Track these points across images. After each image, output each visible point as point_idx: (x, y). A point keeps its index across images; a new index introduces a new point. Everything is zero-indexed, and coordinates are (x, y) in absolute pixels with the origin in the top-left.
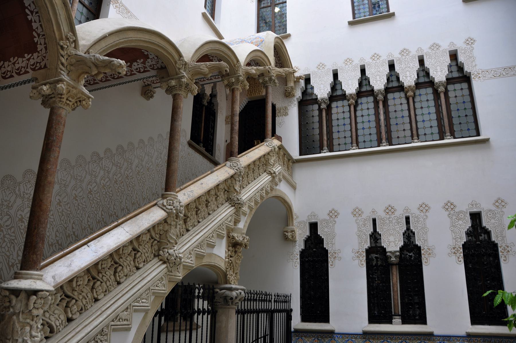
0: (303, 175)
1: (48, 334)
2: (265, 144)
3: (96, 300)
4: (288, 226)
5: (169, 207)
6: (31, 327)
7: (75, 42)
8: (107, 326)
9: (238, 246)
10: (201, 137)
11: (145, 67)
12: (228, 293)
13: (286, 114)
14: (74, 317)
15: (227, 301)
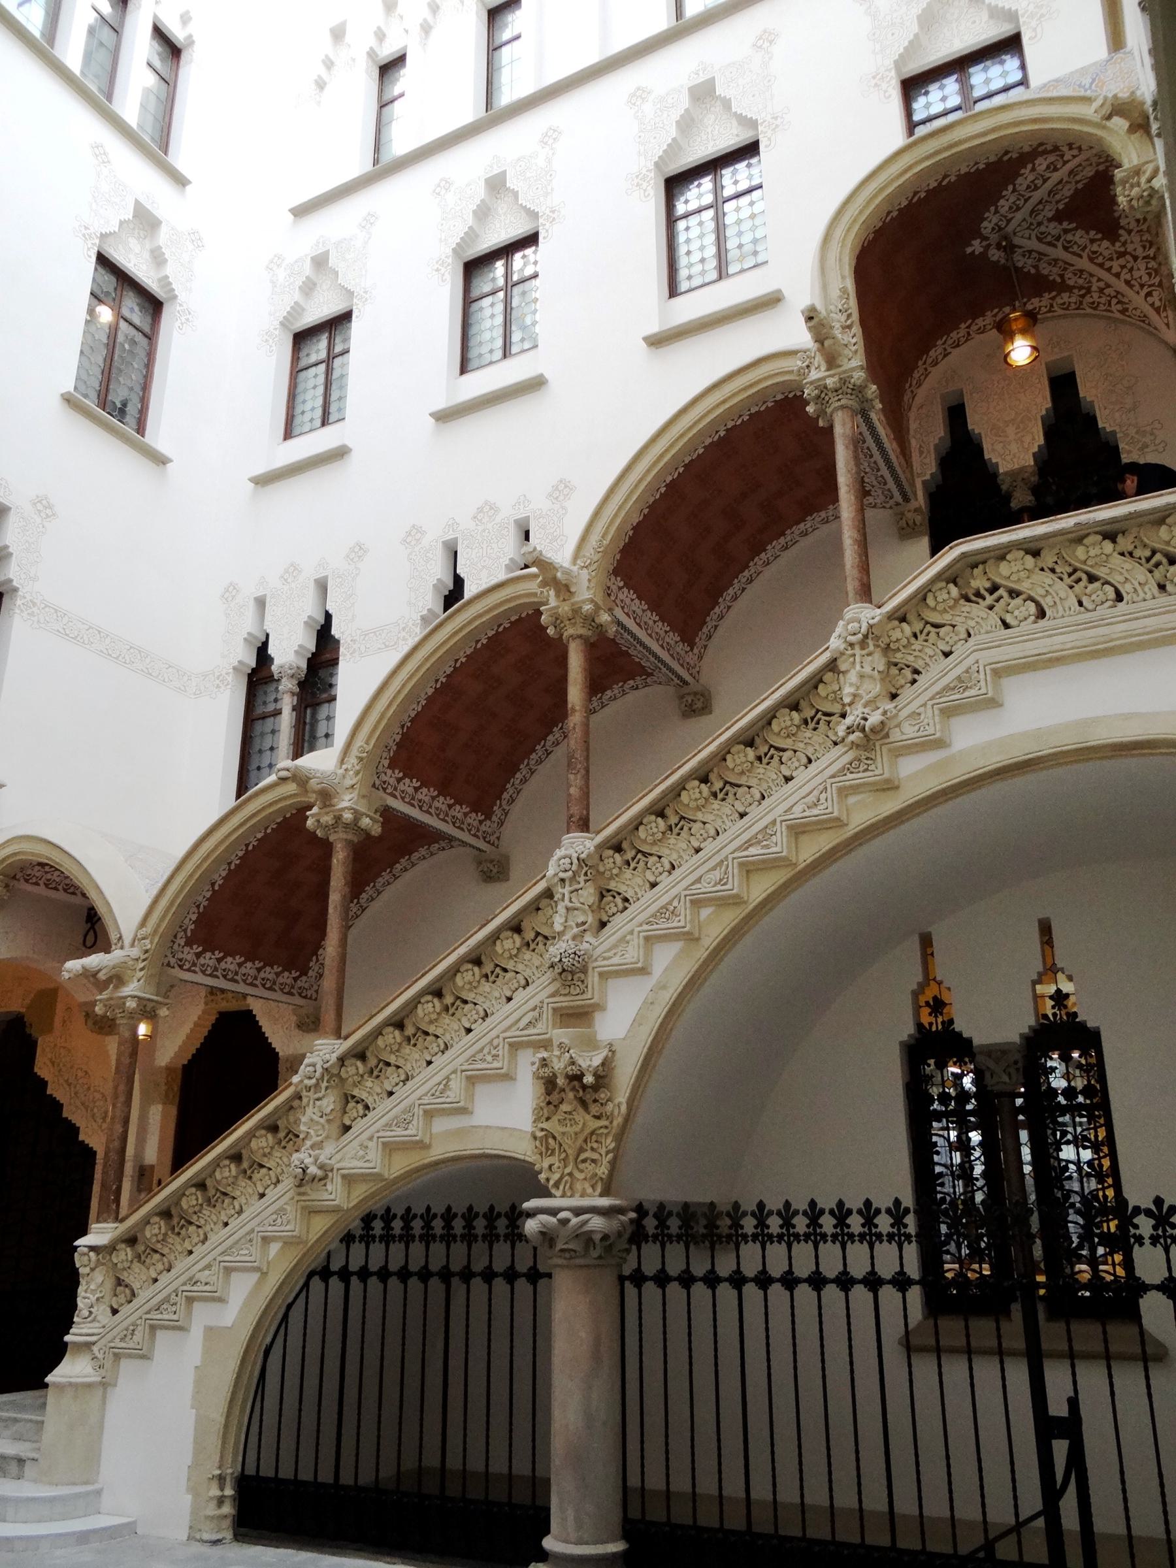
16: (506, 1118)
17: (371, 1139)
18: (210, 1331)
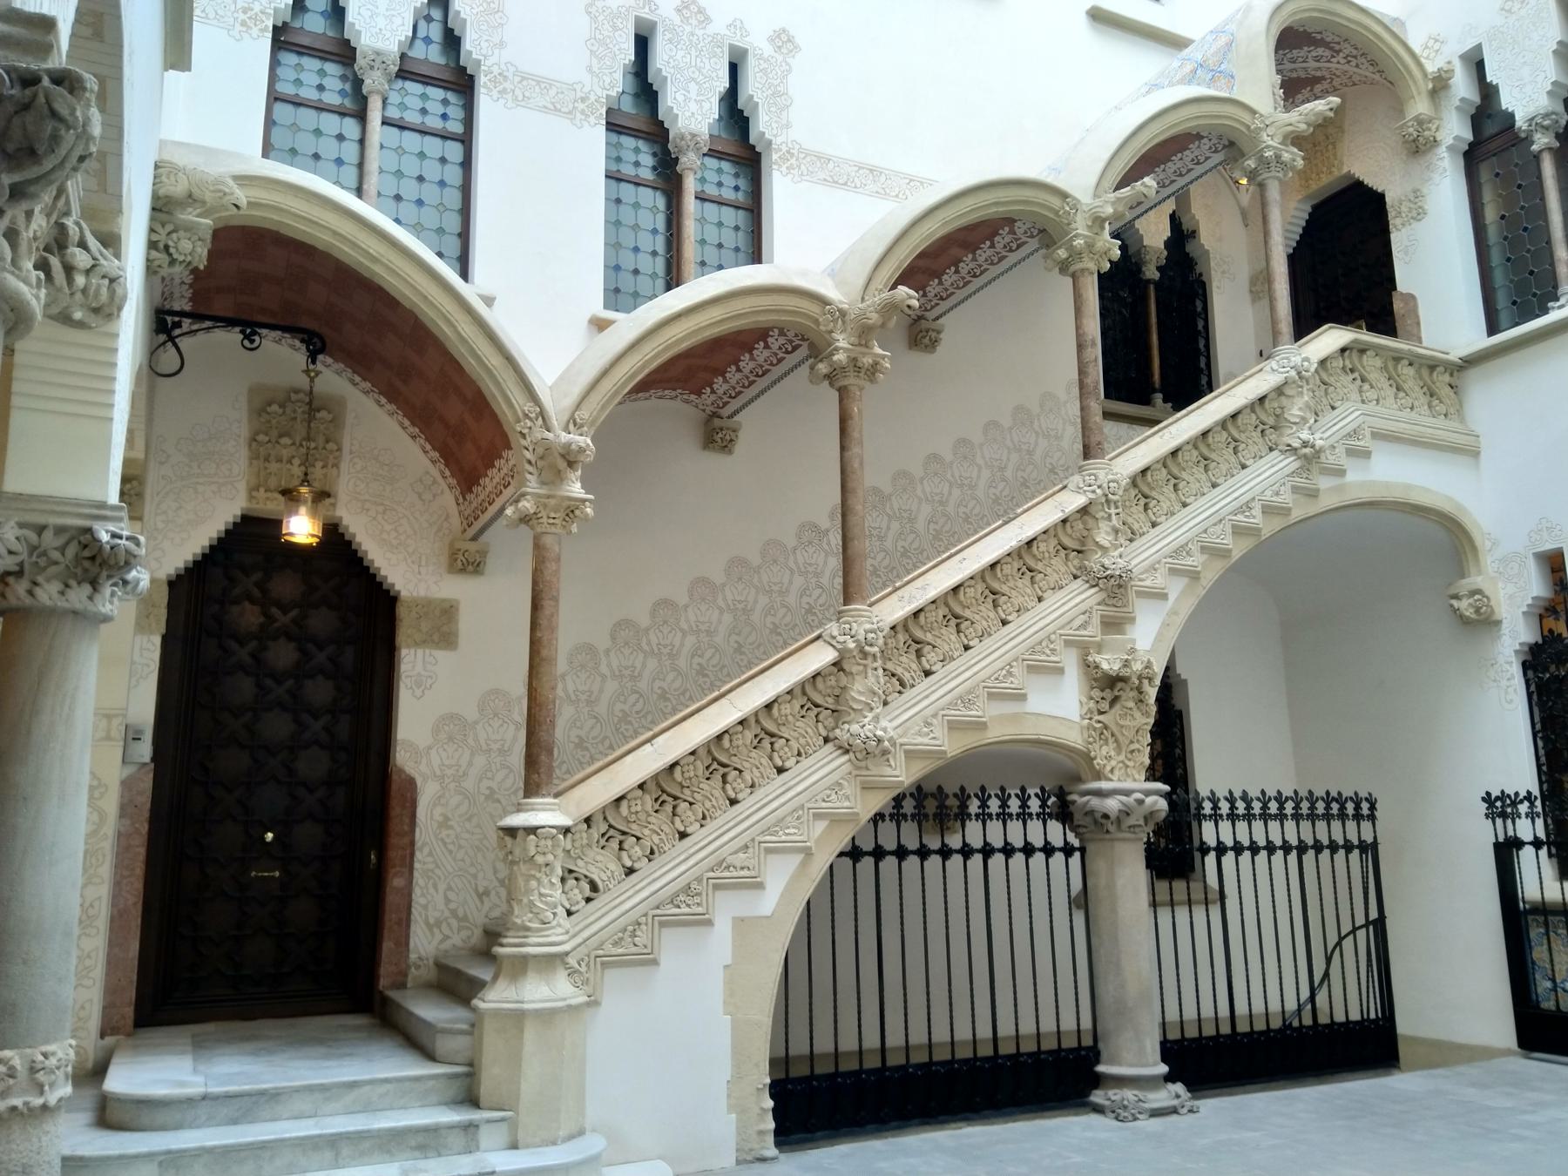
0: (1492, 403)
1: (588, 893)
2: (1268, 368)
3: (683, 835)
4: (1463, 576)
5: (841, 639)
6: (538, 880)
7: (542, 414)
8: (699, 880)
9: (1120, 685)
10: (1152, 376)
11: (791, 342)
12: (1095, 802)
13: (1419, 214)
14: (637, 866)
15: (1101, 821)
16: (1059, 709)
17: (935, 716)
18: (739, 923)
